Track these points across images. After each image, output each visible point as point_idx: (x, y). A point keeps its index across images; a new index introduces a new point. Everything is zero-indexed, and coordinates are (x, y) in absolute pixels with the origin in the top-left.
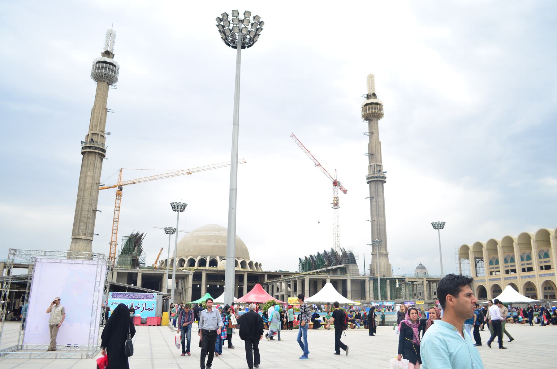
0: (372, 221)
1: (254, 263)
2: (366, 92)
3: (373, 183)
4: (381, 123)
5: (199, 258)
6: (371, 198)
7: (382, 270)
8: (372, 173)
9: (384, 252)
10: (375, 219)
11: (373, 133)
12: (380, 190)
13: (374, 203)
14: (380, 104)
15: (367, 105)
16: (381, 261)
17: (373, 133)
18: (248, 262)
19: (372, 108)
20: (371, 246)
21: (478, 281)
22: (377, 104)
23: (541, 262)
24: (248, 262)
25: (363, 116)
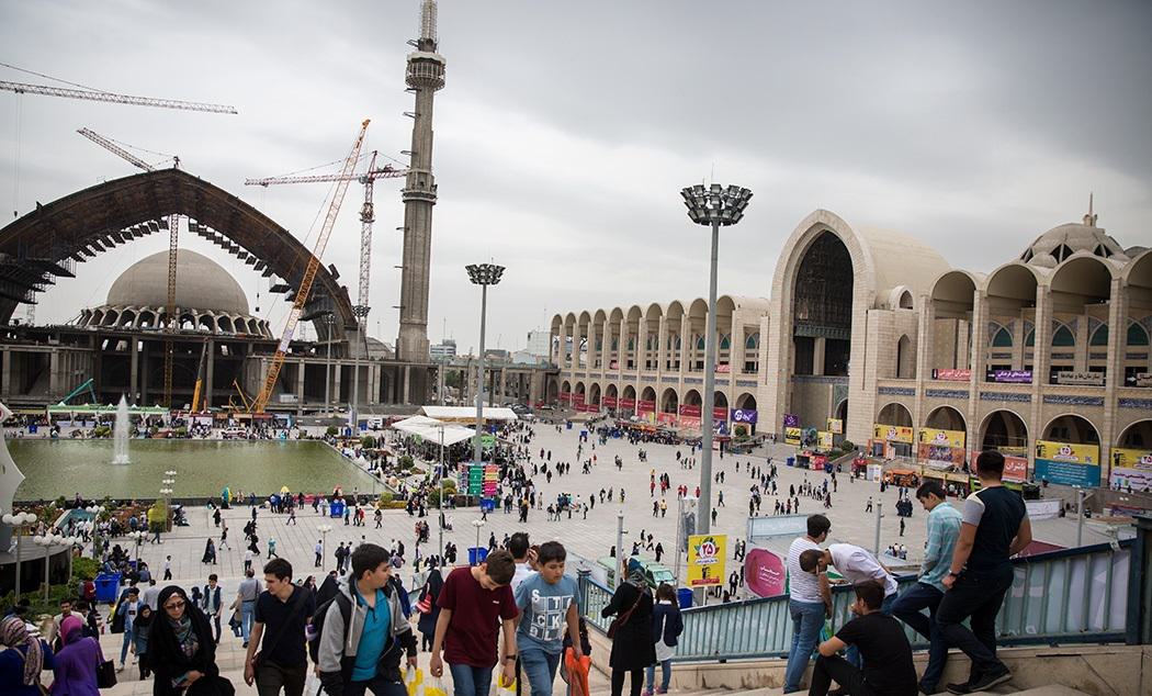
0: (405, 268)
1: (258, 321)
2: (417, 36)
3: (411, 204)
4: (438, 96)
5: (160, 310)
6: (406, 229)
7: (411, 350)
8: (410, 186)
9: (417, 321)
10: (408, 265)
11: (423, 116)
12: (422, 217)
13: (409, 239)
14: (439, 63)
15: (414, 61)
16: (414, 335)
17: (423, 116)
18: (247, 320)
19: (425, 68)
20: (399, 310)
21: (565, 374)
22: (431, 60)
23: (649, 355)
24: (247, 320)
25: (409, 80)
